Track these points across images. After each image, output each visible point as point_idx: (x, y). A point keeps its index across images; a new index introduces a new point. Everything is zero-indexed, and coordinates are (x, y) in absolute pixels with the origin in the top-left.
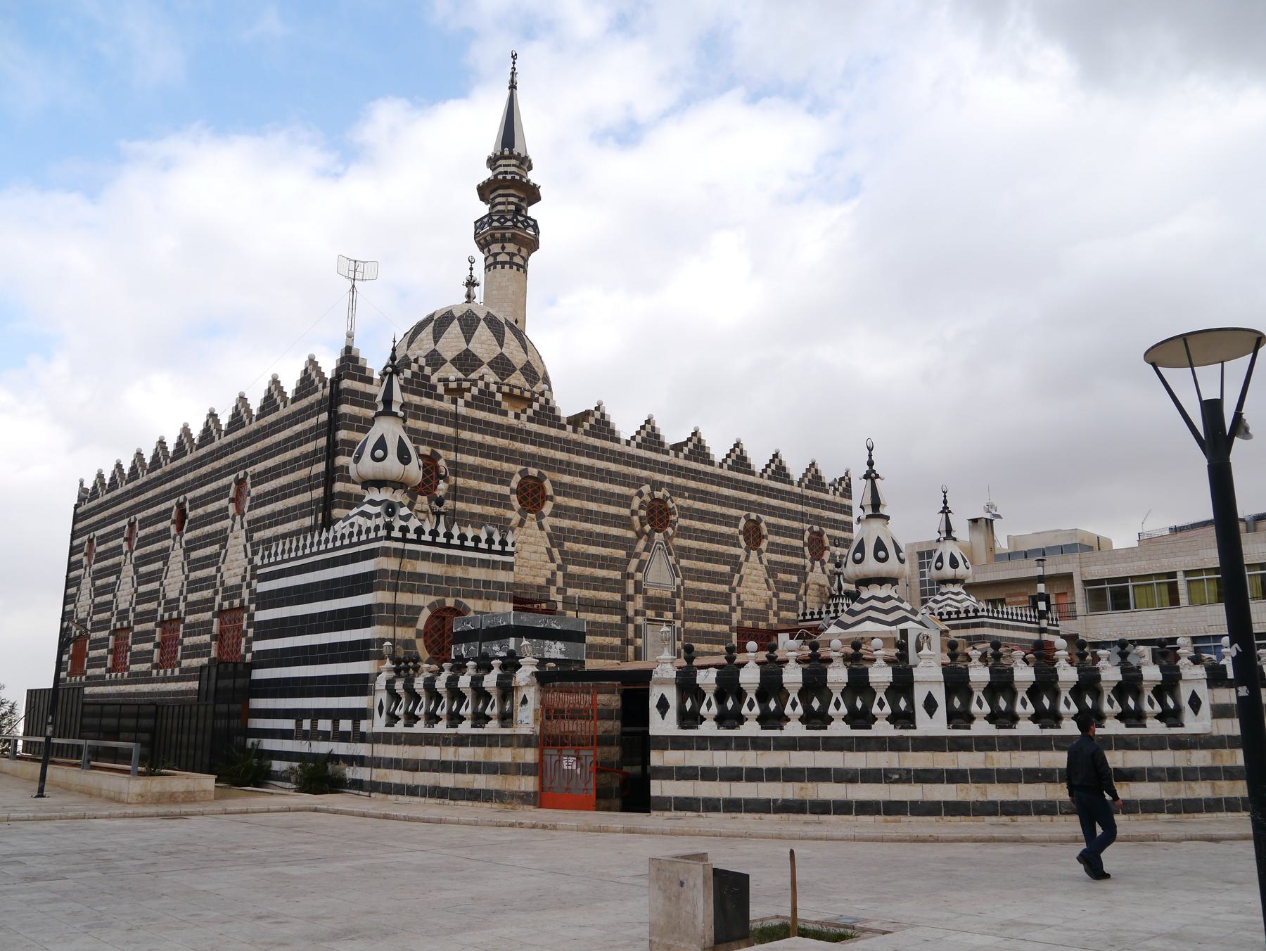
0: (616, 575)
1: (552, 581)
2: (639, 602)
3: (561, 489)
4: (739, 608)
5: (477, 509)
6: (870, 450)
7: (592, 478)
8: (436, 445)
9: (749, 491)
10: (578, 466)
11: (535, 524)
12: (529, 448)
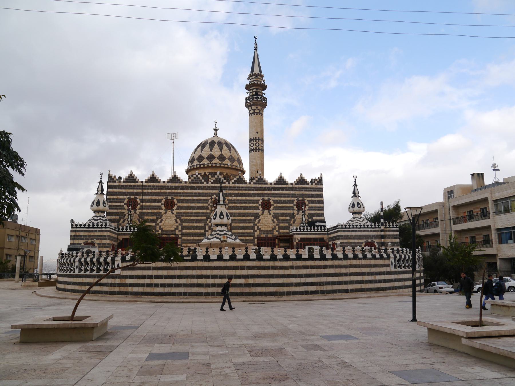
0: (203, 224)
1: (177, 229)
3: (179, 201)
4: (258, 231)
5: (150, 211)
7: (192, 196)
8: (136, 195)
9: (264, 190)
10: (187, 193)
11: (170, 213)
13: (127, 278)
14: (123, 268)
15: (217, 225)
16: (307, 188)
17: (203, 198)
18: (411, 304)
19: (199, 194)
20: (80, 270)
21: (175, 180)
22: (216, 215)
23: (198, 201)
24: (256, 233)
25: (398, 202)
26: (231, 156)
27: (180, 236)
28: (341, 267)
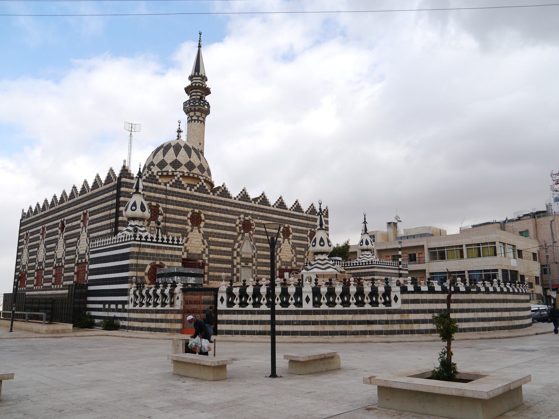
0: (230, 249)
1: (203, 252)
2: (239, 259)
4: (280, 262)
5: (174, 225)
6: (320, 204)
7: (220, 212)
8: (158, 202)
9: (285, 216)
10: (215, 208)
11: (197, 231)
12: (195, 202)
13: (411, 313)
14: (404, 302)
18: (270, 345)
20: (317, 304)
21: (203, 190)
22: (315, 241)
25: (348, 242)
27: (207, 262)
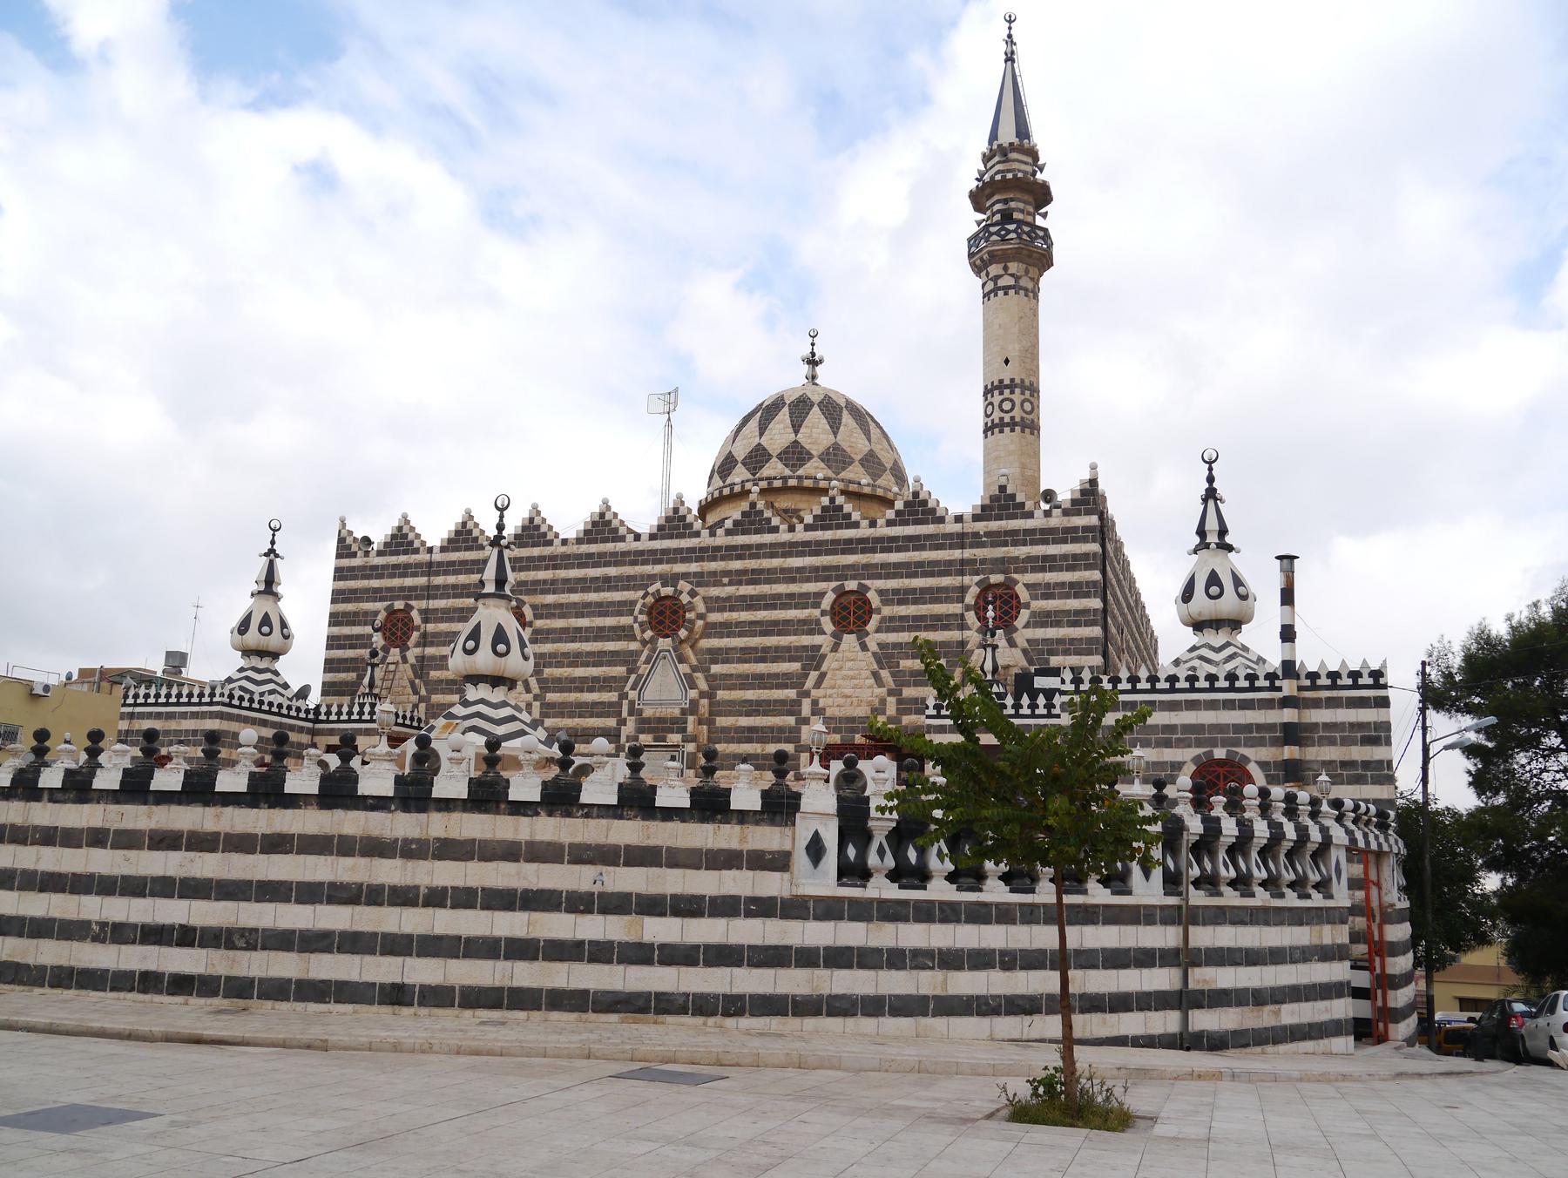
6: (502, 510)
7: (583, 590)
8: (409, 597)
9: (844, 552)
10: (566, 581)
15: (475, 679)
16: (1027, 532)
17: (617, 596)
19: (607, 583)
21: (531, 537)
23: (602, 609)
24: (804, 728)
26: (836, 447)
28: (376, 848)
